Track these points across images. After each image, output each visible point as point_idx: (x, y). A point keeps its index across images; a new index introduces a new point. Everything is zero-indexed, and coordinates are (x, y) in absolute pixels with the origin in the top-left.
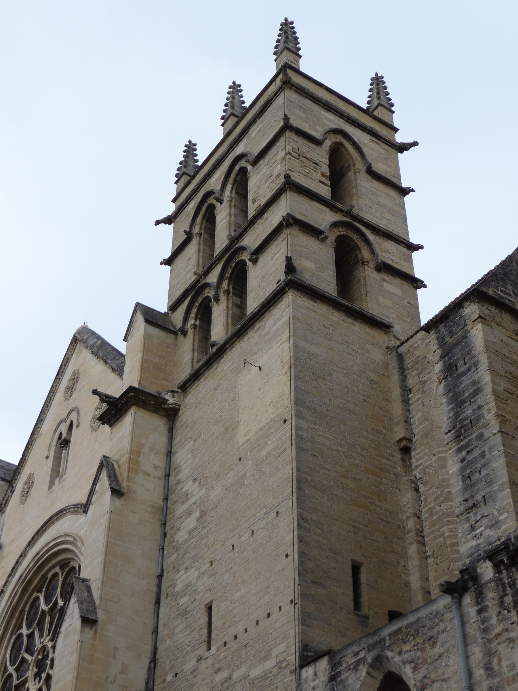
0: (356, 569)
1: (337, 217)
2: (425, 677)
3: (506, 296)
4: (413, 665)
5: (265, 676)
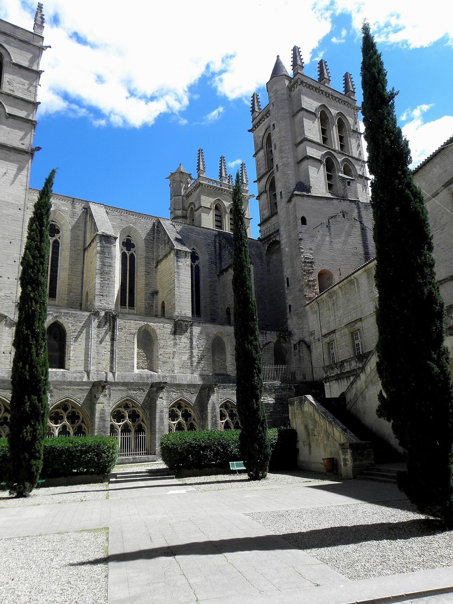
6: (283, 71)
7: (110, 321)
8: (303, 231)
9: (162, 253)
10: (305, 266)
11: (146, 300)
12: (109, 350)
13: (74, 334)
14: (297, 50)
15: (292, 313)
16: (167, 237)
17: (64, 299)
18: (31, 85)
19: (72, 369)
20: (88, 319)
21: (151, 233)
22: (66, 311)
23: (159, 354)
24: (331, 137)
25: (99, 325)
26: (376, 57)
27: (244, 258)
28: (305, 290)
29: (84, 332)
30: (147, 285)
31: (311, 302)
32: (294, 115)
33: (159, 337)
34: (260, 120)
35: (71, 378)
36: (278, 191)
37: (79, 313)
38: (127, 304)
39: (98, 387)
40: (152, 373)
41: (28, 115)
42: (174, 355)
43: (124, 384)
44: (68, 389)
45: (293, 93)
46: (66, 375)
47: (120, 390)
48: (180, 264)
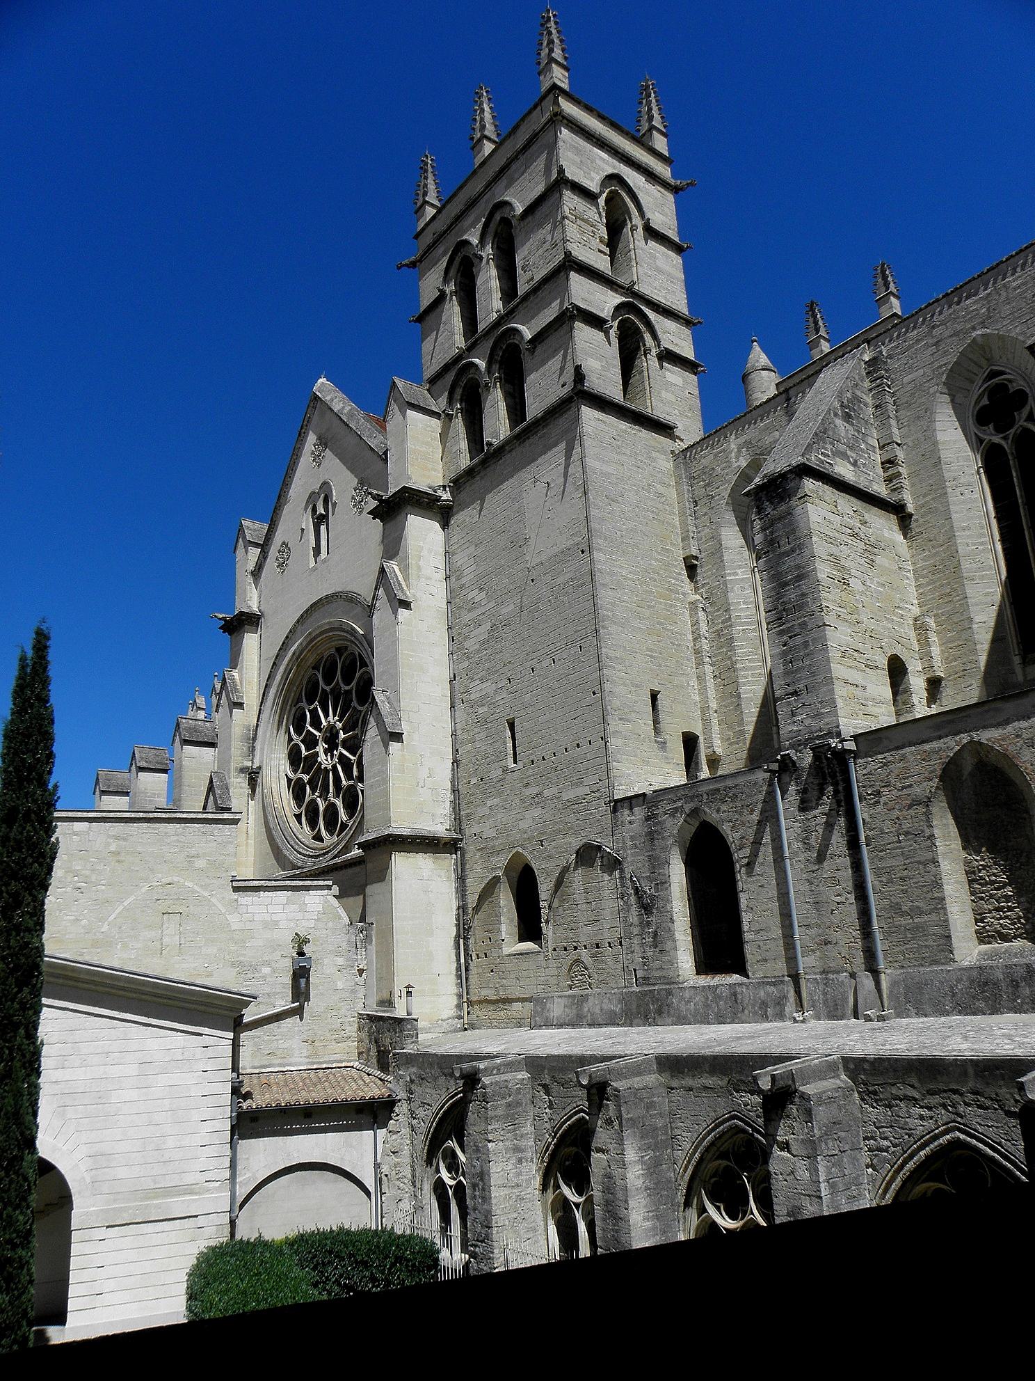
0: (654, 696)
1: (619, 299)
2: (743, 837)
3: (826, 459)
5: (577, 801)
7: (833, 776)
12: (849, 885)
19: (757, 971)
22: (711, 787)
25: (803, 801)
29: (767, 838)
47: (706, 1088)
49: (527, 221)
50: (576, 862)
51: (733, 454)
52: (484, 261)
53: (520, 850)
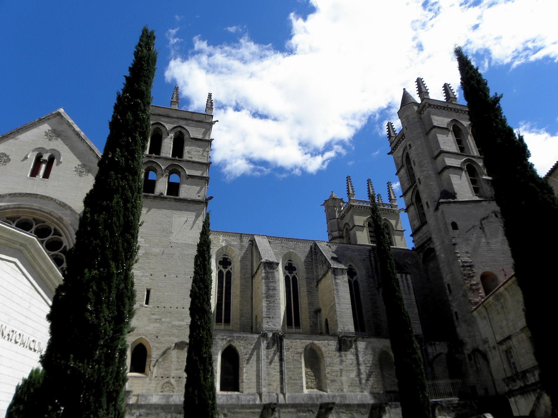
4: (244, 347)
5: (180, 326)
6: (410, 99)
7: (277, 341)
8: (456, 236)
9: (321, 273)
10: (464, 270)
11: (310, 318)
12: (278, 370)
13: (246, 356)
14: (420, 81)
15: (460, 321)
16: (323, 258)
17: (237, 324)
18: (204, 151)
19: (246, 392)
20: (257, 341)
21: (310, 256)
23: (327, 372)
24: (467, 145)
25: (268, 346)
26: (472, 71)
27: (390, 270)
28: (469, 294)
29: (255, 354)
30: (310, 304)
31: (477, 307)
32: (427, 133)
33: (325, 355)
34: (397, 143)
35: (245, 401)
36: (424, 201)
37: (249, 335)
38: (293, 324)
39: (268, 410)
40: (321, 393)
41: (203, 173)
42: (341, 373)
43: (294, 406)
44: (241, 413)
45: (423, 116)
46: (240, 398)
47: (289, 412)
48: (338, 281)
49: (192, 140)
50: (175, 347)
51: (221, 241)
52: (169, 137)
53: (144, 337)
